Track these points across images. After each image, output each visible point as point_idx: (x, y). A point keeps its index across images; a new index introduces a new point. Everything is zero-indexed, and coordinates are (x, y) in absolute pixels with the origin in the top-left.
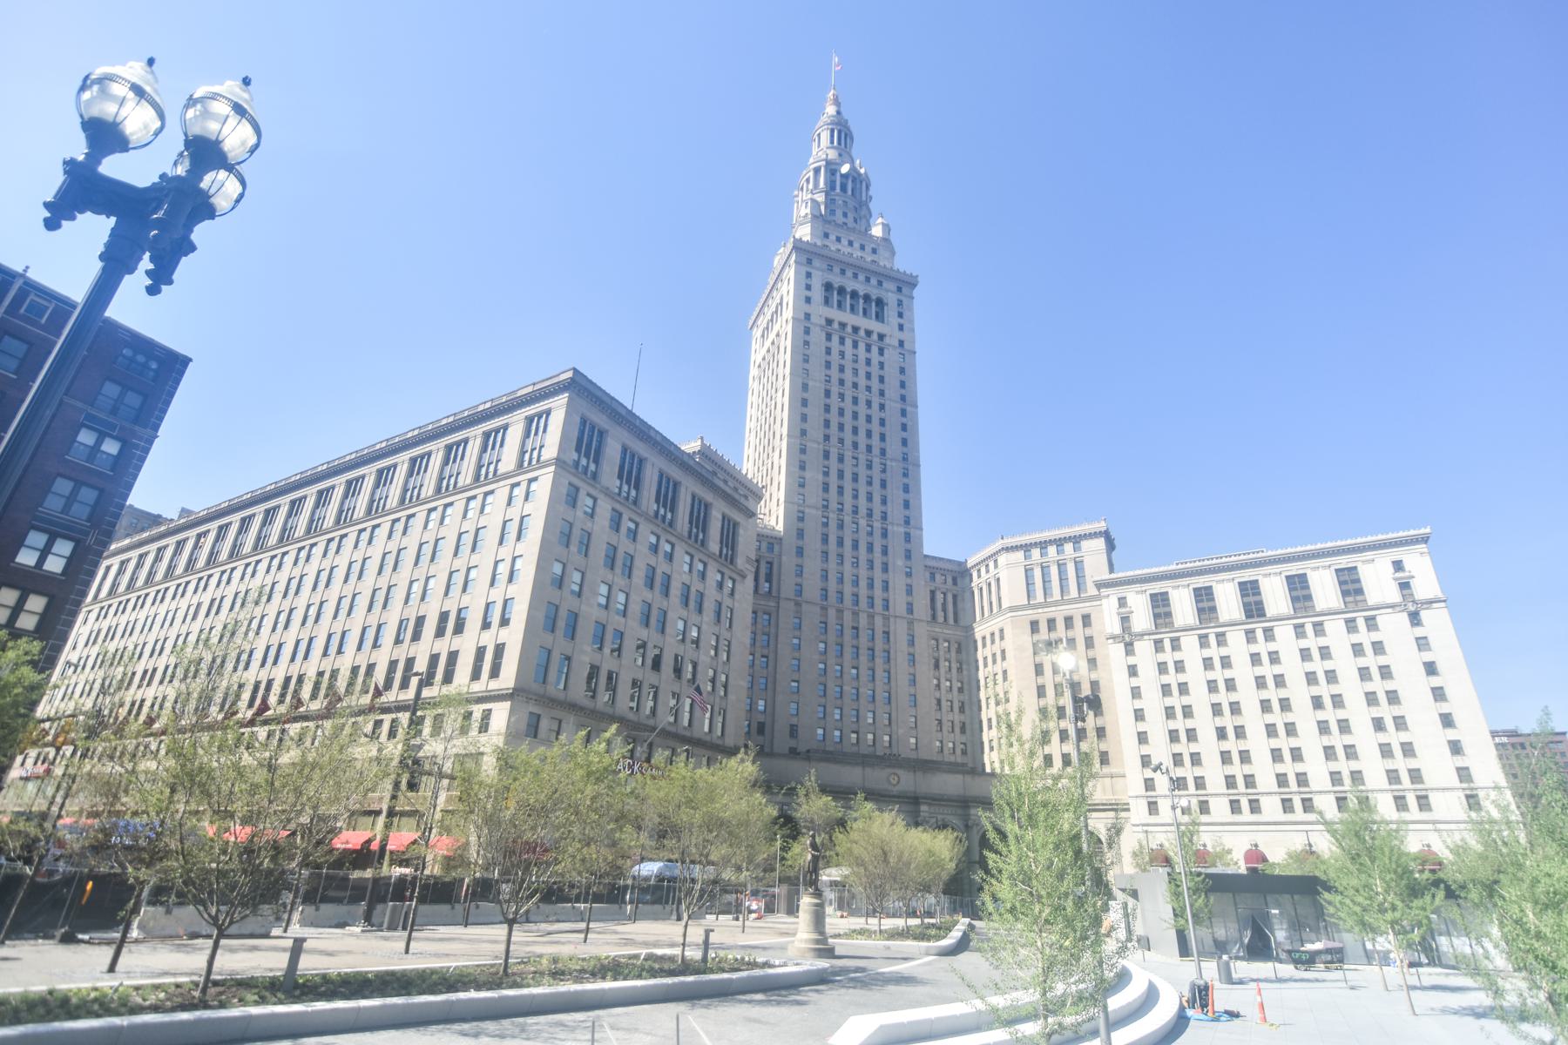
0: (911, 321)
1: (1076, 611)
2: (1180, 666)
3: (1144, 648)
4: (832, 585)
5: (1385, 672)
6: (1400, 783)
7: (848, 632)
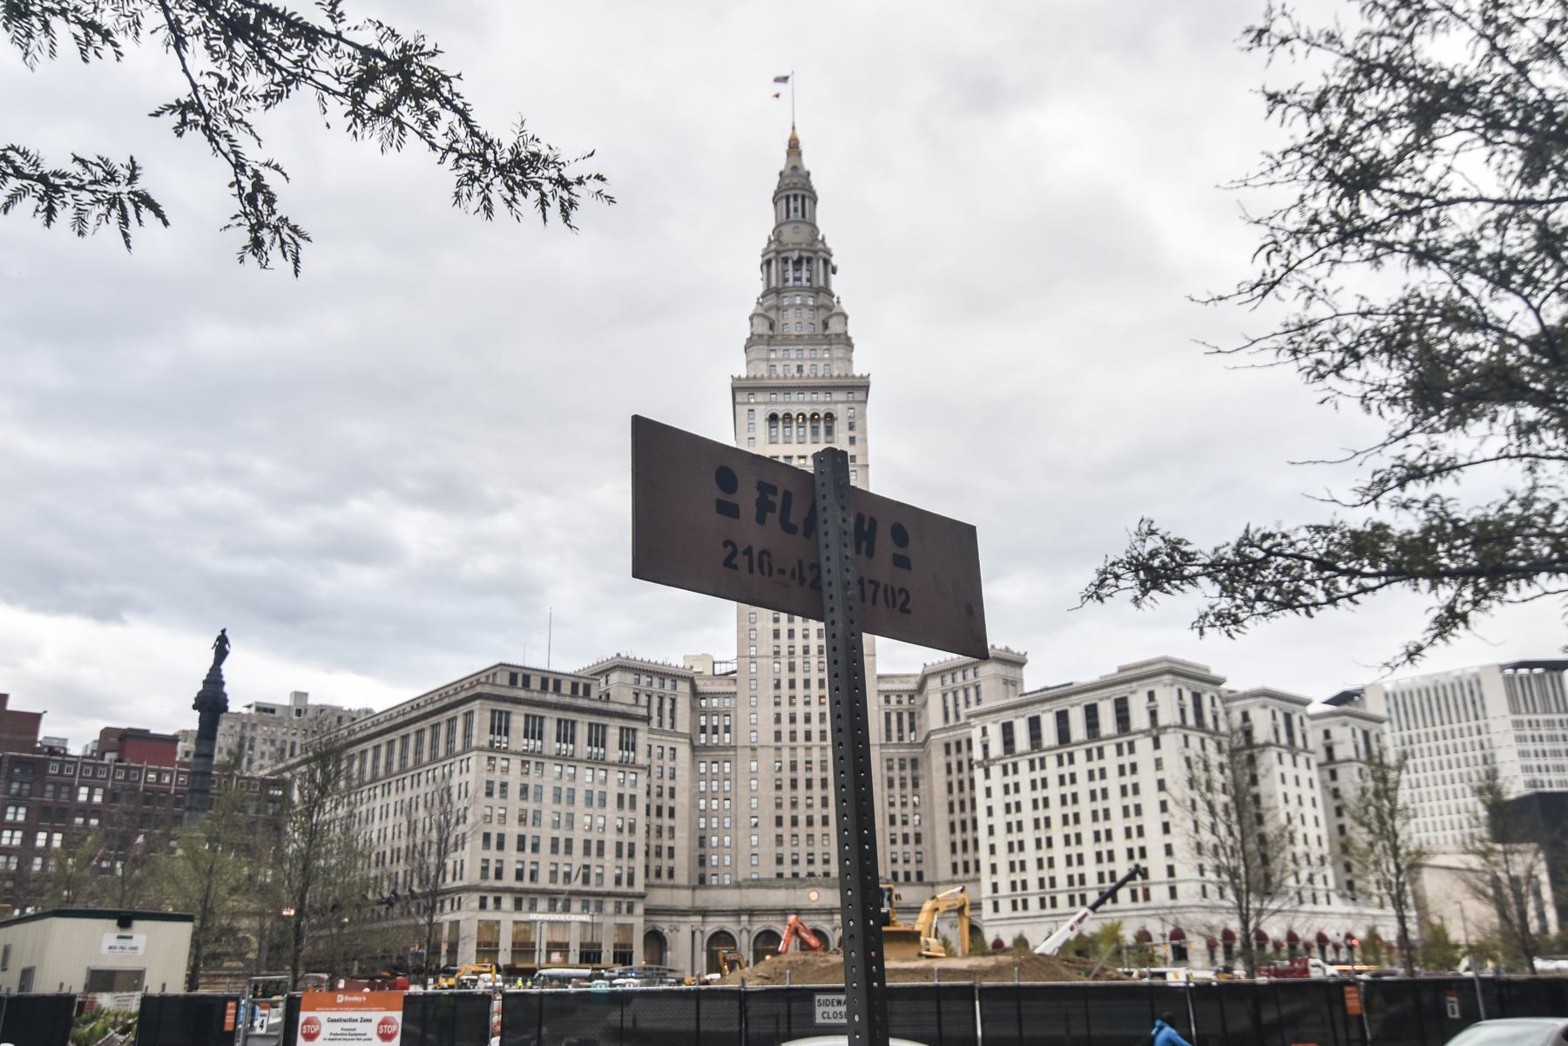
0: (864, 431)
4: (785, 727)
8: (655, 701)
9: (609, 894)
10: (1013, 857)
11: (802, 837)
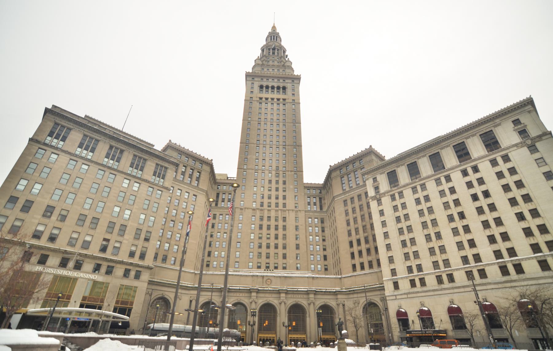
0: (298, 92)
1: (360, 191)
2: (404, 206)
3: (386, 200)
5: (520, 184)
6: (541, 251)
7: (265, 218)
8: (189, 171)
9: (122, 263)
10: (406, 250)
11: (264, 255)
